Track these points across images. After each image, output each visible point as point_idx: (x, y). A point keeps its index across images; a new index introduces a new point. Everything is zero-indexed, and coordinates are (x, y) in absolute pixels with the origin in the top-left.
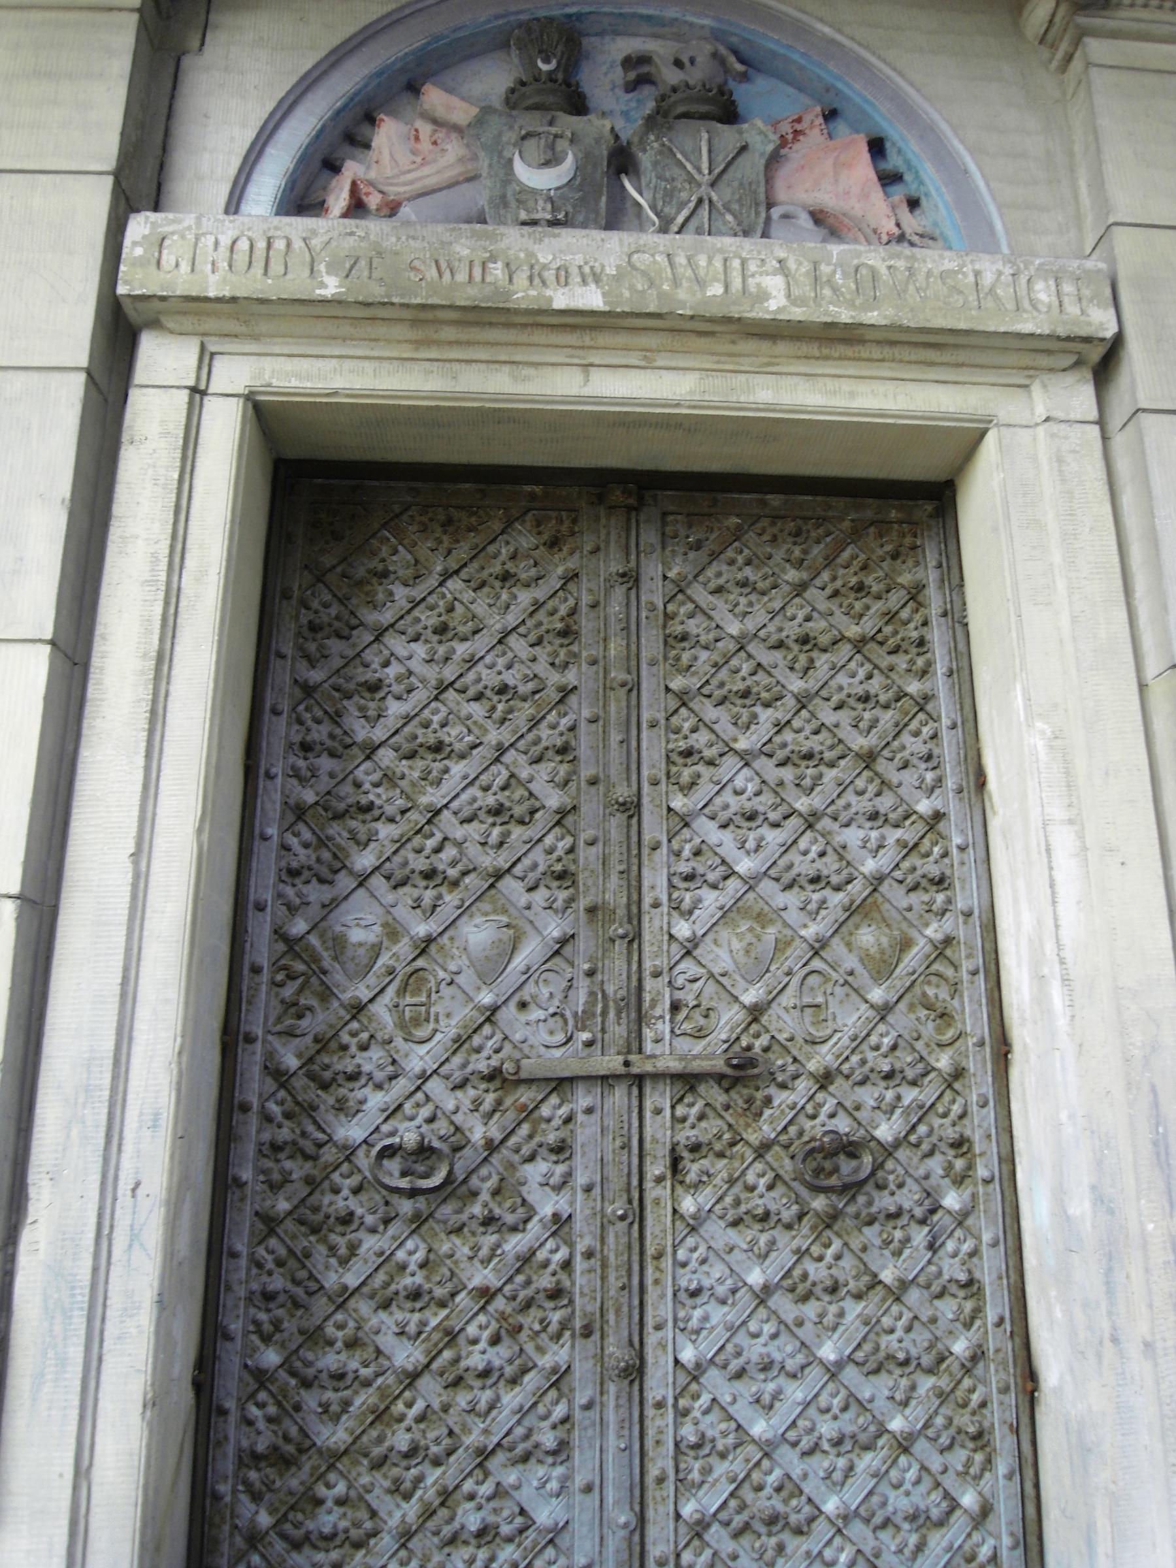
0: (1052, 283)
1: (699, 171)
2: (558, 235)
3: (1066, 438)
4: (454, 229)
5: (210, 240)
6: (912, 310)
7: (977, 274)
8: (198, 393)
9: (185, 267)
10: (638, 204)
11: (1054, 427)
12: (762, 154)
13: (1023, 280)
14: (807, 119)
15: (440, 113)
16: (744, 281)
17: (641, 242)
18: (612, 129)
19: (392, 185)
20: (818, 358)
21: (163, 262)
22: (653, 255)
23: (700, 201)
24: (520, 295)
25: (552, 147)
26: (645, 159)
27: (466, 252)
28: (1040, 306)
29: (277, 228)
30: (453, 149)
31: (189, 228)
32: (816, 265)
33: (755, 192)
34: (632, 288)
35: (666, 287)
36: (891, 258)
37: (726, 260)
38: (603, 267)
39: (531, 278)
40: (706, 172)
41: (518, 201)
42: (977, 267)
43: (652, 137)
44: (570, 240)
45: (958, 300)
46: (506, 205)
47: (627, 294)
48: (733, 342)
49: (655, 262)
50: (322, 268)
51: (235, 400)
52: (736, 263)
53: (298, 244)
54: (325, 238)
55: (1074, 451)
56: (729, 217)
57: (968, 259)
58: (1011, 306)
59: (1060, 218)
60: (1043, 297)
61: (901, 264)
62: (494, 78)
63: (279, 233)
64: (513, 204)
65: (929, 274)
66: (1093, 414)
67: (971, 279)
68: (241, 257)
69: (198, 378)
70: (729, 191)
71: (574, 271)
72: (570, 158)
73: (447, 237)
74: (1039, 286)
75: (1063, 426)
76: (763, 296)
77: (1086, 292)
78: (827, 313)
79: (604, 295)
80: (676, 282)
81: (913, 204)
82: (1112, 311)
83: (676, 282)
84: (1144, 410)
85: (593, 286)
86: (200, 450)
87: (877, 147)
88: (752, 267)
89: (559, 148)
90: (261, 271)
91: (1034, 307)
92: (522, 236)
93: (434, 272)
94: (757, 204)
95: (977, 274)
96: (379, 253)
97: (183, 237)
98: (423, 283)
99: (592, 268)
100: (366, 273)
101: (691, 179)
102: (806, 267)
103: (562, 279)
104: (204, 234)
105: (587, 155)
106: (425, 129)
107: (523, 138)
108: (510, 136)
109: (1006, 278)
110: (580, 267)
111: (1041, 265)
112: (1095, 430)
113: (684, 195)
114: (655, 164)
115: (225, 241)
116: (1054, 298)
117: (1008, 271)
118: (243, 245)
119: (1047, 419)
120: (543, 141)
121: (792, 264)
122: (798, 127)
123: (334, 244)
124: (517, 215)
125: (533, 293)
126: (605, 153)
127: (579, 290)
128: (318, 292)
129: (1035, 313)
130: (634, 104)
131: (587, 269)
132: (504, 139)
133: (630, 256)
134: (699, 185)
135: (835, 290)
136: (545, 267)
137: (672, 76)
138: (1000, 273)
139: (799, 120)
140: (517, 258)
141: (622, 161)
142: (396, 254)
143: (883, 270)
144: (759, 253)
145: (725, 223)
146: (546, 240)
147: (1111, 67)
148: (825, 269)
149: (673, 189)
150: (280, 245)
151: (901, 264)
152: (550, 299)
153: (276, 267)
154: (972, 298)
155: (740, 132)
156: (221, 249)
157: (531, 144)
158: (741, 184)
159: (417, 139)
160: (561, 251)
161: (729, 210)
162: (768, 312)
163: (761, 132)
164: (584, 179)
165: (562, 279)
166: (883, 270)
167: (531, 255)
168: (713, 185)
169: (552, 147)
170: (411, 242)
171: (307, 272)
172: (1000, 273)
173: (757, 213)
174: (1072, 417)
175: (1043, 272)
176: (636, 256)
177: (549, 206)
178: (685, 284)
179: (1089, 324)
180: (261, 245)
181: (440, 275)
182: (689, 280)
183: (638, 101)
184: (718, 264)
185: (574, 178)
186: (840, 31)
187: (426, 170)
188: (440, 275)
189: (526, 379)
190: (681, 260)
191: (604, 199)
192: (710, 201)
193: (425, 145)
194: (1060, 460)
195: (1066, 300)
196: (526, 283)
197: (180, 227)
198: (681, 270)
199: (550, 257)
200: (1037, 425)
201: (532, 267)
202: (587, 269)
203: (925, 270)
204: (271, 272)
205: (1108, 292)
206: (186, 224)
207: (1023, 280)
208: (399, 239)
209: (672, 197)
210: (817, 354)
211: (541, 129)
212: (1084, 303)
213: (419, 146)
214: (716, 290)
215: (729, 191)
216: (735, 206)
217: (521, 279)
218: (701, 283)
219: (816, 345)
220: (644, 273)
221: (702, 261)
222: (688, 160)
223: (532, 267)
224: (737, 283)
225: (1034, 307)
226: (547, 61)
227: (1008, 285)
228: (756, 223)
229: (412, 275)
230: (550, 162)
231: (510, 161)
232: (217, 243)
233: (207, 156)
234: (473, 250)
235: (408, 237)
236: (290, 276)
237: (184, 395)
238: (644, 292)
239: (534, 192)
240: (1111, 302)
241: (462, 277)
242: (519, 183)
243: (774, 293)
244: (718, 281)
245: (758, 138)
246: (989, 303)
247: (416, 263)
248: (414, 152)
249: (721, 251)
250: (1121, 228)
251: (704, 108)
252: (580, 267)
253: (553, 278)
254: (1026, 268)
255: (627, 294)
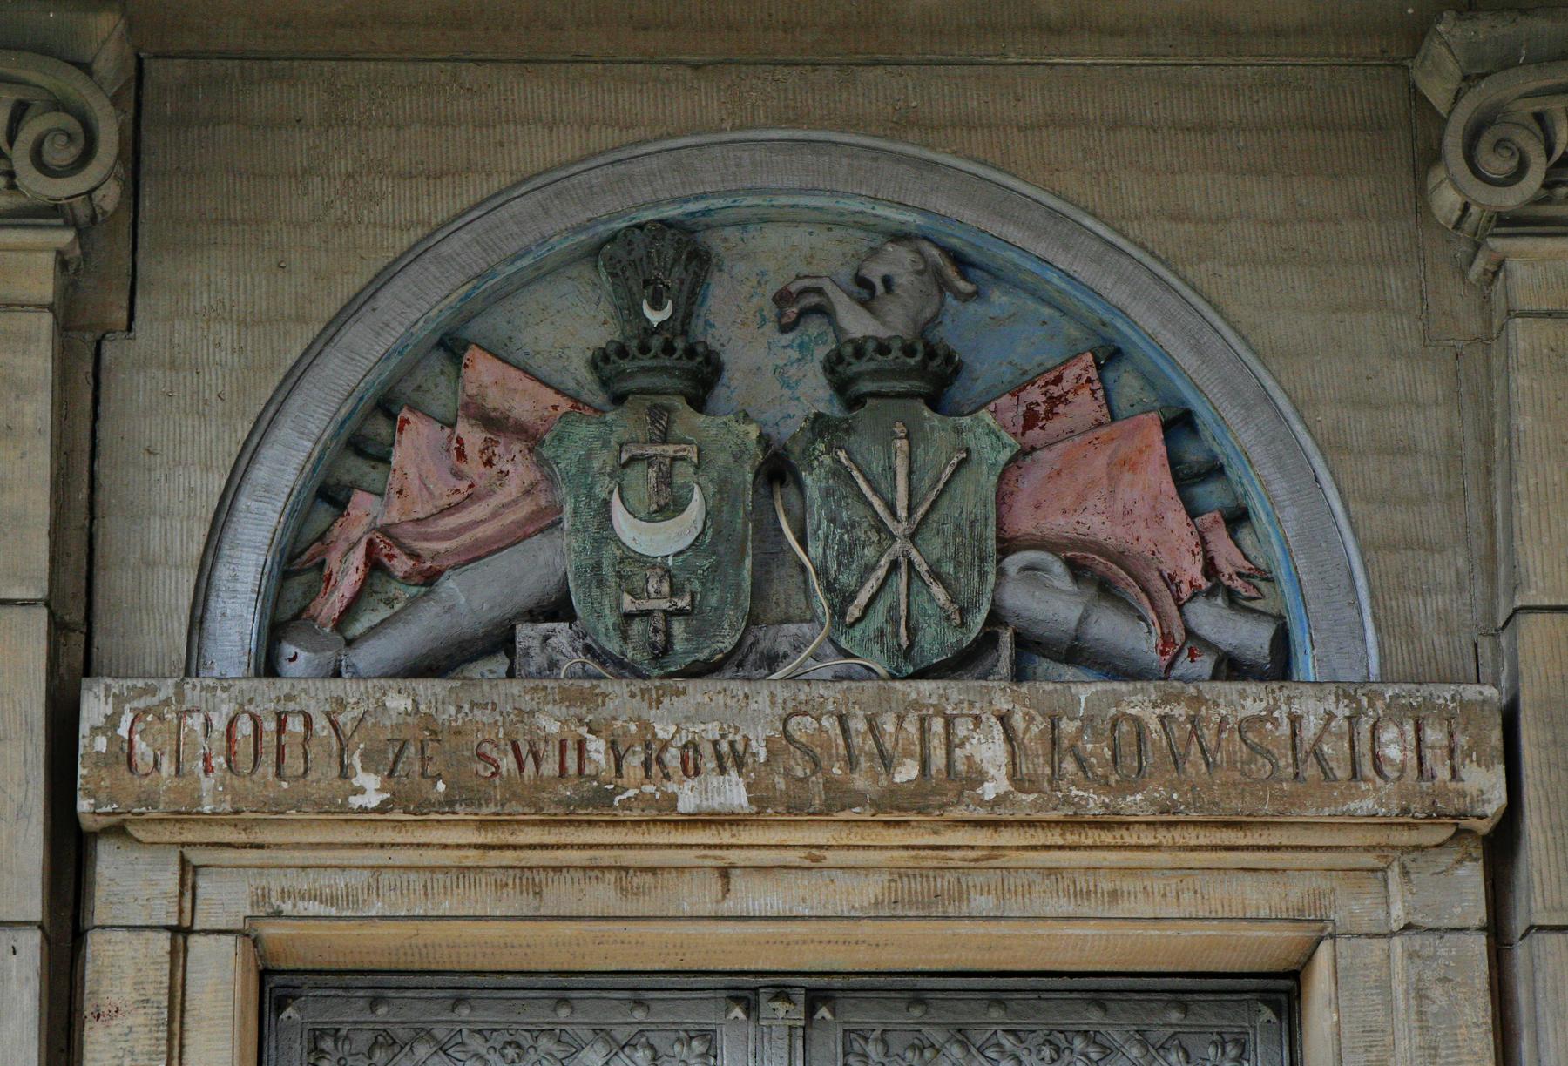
0: (1409, 728)
1: (894, 514)
2: (684, 692)
3: (1435, 957)
4: (535, 689)
5: (196, 722)
6: (1193, 787)
7: (1295, 720)
8: (181, 932)
9: (167, 768)
10: (803, 568)
11: (1417, 941)
12: (992, 466)
13: (1365, 727)
14: (1070, 375)
15: (494, 400)
16: (949, 753)
17: (802, 697)
18: (760, 436)
19: (427, 537)
20: (1061, 848)
21: (137, 759)
22: (818, 720)
23: (894, 566)
24: (631, 793)
25: (666, 479)
26: (813, 482)
27: (554, 728)
28: (1387, 769)
29: (289, 698)
30: (518, 469)
31: (167, 702)
32: (1054, 726)
33: (980, 539)
34: (788, 773)
35: (836, 771)
36: (1166, 701)
37: (922, 720)
38: (747, 740)
39: (646, 766)
40: (902, 513)
41: (619, 575)
42: (1295, 708)
43: (822, 447)
44: (699, 698)
45: (1262, 767)
46: (601, 583)
47: (781, 783)
48: (936, 833)
49: (821, 729)
50: (356, 761)
51: (230, 939)
52: (938, 725)
53: (321, 725)
54: (358, 712)
55: (1445, 980)
56: (938, 591)
57: (1282, 696)
58: (1342, 772)
59: (1460, 562)
60: (1393, 752)
61: (1180, 711)
62: (572, 324)
63: (291, 706)
64: (612, 581)
65: (1223, 721)
66: (1477, 913)
67: (1285, 728)
68: (244, 748)
69: (181, 912)
70: (938, 541)
71: (707, 750)
72: (697, 495)
73: (527, 703)
74: (1389, 734)
75: (1430, 939)
76: (977, 777)
77: (1462, 740)
78: (1067, 801)
79: (749, 787)
80: (851, 762)
81: (1237, 518)
82: (1500, 769)
83: (851, 762)
84: (1541, 928)
85: (734, 774)
86: (188, 1020)
87: (1179, 423)
88: (962, 728)
89: (678, 481)
90: (272, 770)
91: (1379, 771)
92: (633, 695)
93: (508, 763)
94: (982, 560)
95: (1295, 720)
96: (434, 732)
97: (161, 718)
98: (497, 781)
99: (732, 744)
100: (417, 767)
101: (880, 526)
102: (1040, 724)
103: (691, 765)
104: (189, 712)
105: (722, 486)
106: (473, 437)
107: (625, 466)
108: (603, 460)
109: (1340, 724)
110: (715, 743)
111: (1398, 696)
112: (1478, 945)
113: (869, 553)
114: (827, 493)
115: (219, 723)
116: (1412, 756)
117: (1342, 711)
118: (245, 727)
119: (1408, 927)
120: (652, 474)
121: (1018, 721)
122: (1055, 391)
123: (370, 721)
124: (619, 605)
125: (649, 788)
126: (750, 477)
127: (715, 780)
128: (352, 799)
129: (1379, 782)
130: (795, 354)
131: (725, 747)
132: (596, 465)
133: (785, 722)
134: (893, 538)
135: (1080, 762)
136: (665, 745)
137: (857, 323)
138: (1330, 716)
139: (1057, 380)
140: (626, 732)
141: (777, 470)
142: (458, 732)
143: (1154, 725)
144: (972, 704)
145: (932, 599)
146: (666, 701)
147: (1549, 314)
148: (1068, 727)
149: (854, 542)
150: (295, 725)
151: (1180, 711)
152: (673, 799)
153: (294, 764)
154: (1285, 761)
155: (958, 431)
156: (215, 735)
157: (635, 474)
158: (958, 527)
159: (461, 454)
160: (687, 718)
161: (937, 575)
162: (981, 803)
163: (991, 432)
164: (718, 533)
165: (691, 765)
166: (1154, 725)
167: (645, 726)
168: (912, 537)
169: (666, 479)
170: (476, 711)
171: (335, 771)
172: (1330, 716)
173: (983, 575)
174: (1445, 923)
175: (1396, 710)
176: (794, 721)
177: (666, 588)
178: (864, 763)
179: (1462, 794)
180: (270, 726)
181: (521, 767)
182: (870, 756)
183: (801, 346)
184: (911, 727)
185: (703, 533)
186: (1121, 232)
187: (478, 511)
188: (521, 767)
189: (638, 892)
190: (858, 725)
191: (748, 562)
192: (910, 563)
193: (473, 467)
194: (1421, 996)
195: (1428, 754)
196: (641, 773)
197: (155, 700)
198: (857, 741)
199: (673, 729)
200: (1393, 934)
201: (648, 746)
202: (725, 747)
203: (1216, 719)
204: (287, 772)
205: (1496, 737)
206: (162, 695)
207: (1365, 727)
208: (460, 708)
209: (851, 554)
210: (1060, 842)
211: (651, 450)
212: (1458, 759)
213: (463, 467)
214: (907, 772)
215: (938, 541)
216: (948, 568)
217: (634, 762)
218: (887, 761)
219: (1058, 831)
220: (806, 750)
221: (890, 727)
222: (875, 491)
223: (648, 746)
224: (938, 759)
225: (1379, 771)
226: (657, 305)
227: (1340, 737)
228: (980, 593)
229: (480, 767)
230: (670, 508)
231: (606, 503)
232: (208, 722)
233: (156, 523)
234: (564, 723)
235: (473, 705)
236: (312, 776)
237: (163, 941)
238: (804, 780)
239: (642, 560)
240: (1499, 753)
241: (550, 768)
242: (621, 544)
243: (992, 771)
244: (911, 756)
245: (986, 441)
246: (1311, 770)
247: (487, 748)
248: (458, 475)
249: (916, 705)
250: (1532, 617)
251: (901, 386)
252: (715, 743)
253: (677, 764)
254: (1371, 704)
255: (781, 783)
